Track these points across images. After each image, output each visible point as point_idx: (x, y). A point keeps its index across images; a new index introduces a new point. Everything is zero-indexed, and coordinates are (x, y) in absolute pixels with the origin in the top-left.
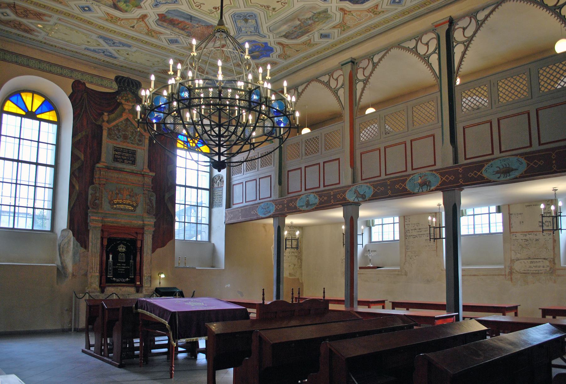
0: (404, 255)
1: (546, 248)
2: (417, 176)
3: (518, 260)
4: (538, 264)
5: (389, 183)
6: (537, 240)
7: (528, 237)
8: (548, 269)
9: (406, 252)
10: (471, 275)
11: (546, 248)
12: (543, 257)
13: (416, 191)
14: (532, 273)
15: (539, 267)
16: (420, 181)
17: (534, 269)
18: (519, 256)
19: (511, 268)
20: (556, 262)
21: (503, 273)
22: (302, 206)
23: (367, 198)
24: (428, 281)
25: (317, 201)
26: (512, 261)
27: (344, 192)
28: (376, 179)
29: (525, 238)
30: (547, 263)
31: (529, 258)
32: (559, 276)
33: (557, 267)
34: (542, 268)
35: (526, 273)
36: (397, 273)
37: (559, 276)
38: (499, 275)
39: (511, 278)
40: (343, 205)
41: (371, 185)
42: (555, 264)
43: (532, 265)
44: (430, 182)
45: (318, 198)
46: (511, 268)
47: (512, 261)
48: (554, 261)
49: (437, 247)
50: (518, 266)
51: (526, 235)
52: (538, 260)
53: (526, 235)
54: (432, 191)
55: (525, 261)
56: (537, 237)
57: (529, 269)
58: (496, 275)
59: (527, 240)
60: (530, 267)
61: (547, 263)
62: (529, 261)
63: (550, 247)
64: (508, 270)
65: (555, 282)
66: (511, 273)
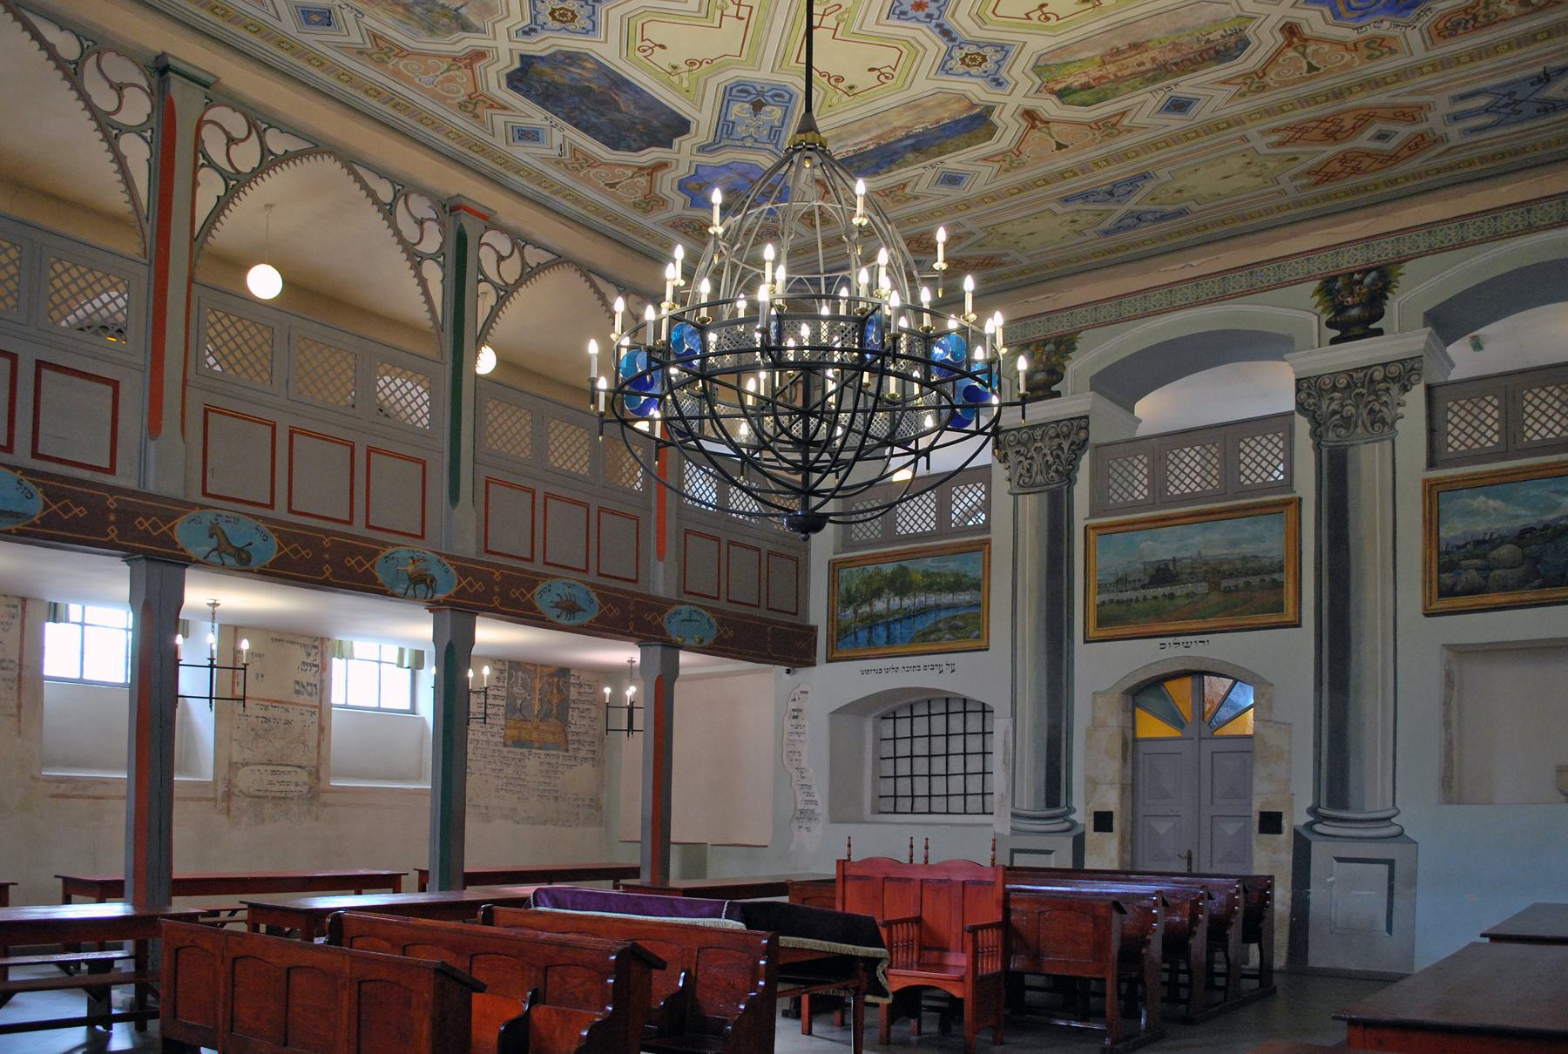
1: (304, 743)
2: (402, 553)
4: (287, 778)
5: (327, 542)
6: (288, 722)
7: (271, 713)
8: (305, 789)
11: (304, 743)
13: (400, 590)
15: (289, 783)
16: (411, 568)
17: (278, 787)
18: (248, 754)
20: (322, 774)
23: (254, 565)
25: (35, 506)
26: (233, 766)
27: (171, 518)
28: (86, 475)
30: (303, 776)
31: (270, 763)
32: (325, 805)
33: (322, 785)
34: (293, 788)
37: (325, 805)
40: (130, 555)
42: (318, 779)
43: (274, 778)
44: (433, 579)
47: (233, 766)
48: (318, 772)
51: (266, 708)
53: (266, 708)
54: (251, 571)
56: (285, 716)
58: (192, 799)
59: (267, 720)
60: (271, 783)
61: (303, 776)
63: (312, 743)
64: (221, 789)
65: (317, 819)
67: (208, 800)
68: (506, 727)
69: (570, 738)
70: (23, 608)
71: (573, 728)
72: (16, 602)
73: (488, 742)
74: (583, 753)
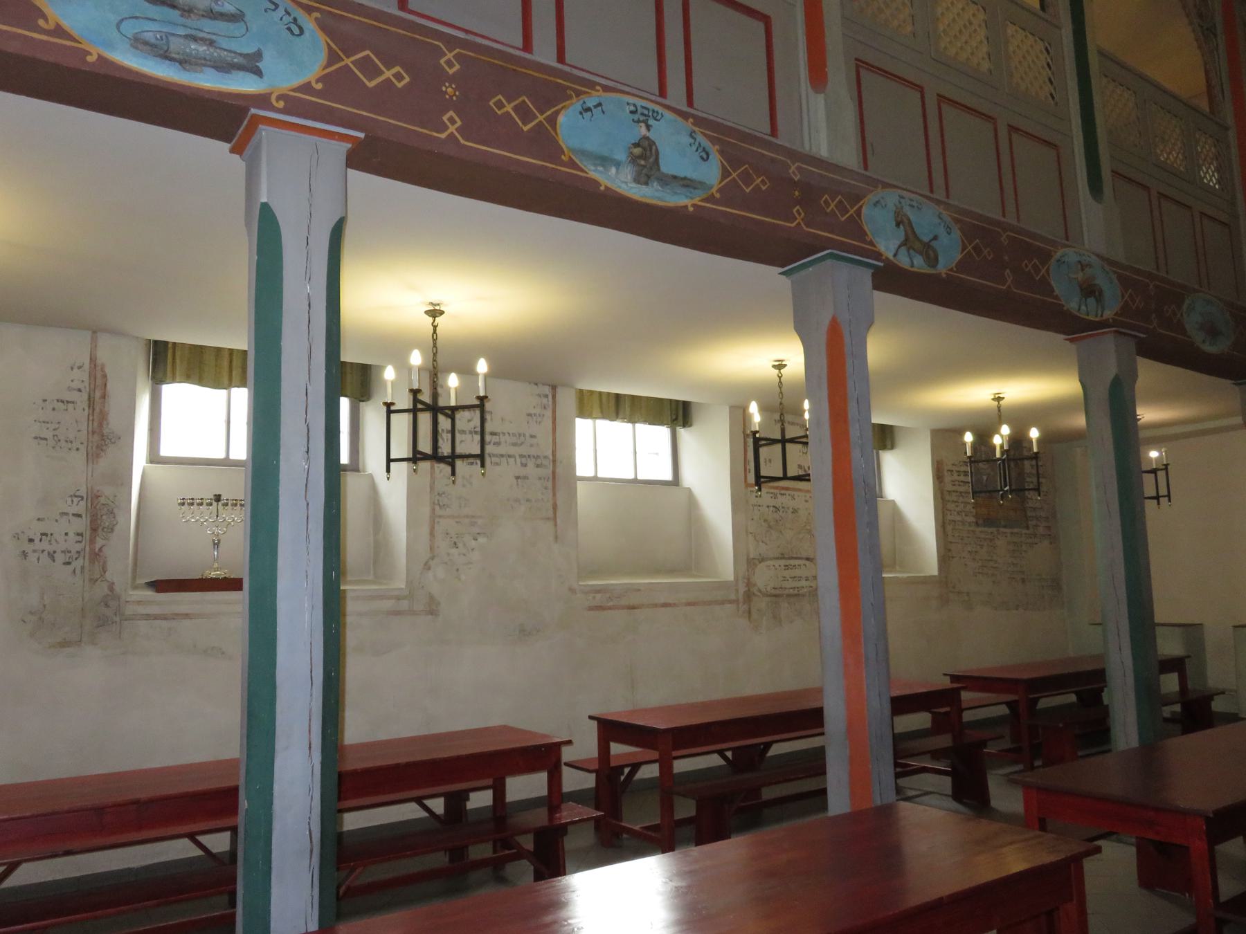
0: (425, 530)
3: (762, 560)
4: (797, 572)
6: (795, 511)
9: (434, 519)
10: (656, 606)
12: (804, 555)
14: (789, 596)
19: (749, 584)
21: (733, 597)
22: (604, 161)
24: (524, 633)
26: (752, 563)
29: (772, 502)
31: (782, 557)
34: (803, 583)
35: (776, 596)
36: (388, 604)
38: (722, 603)
39: (750, 612)
41: (957, 221)
43: (787, 573)
45: (716, 159)
46: (749, 584)
49: (555, 507)
50: (765, 578)
52: (797, 562)
55: (777, 563)
57: (786, 584)
59: (776, 509)
62: (783, 562)
66: (749, 596)
67: (730, 602)
68: (976, 506)
69: (1029, 514)
70: (554, 397)
71: (1030, 504)
72: (547, 390)
73: (963, 522)
74: (1041, 530)
